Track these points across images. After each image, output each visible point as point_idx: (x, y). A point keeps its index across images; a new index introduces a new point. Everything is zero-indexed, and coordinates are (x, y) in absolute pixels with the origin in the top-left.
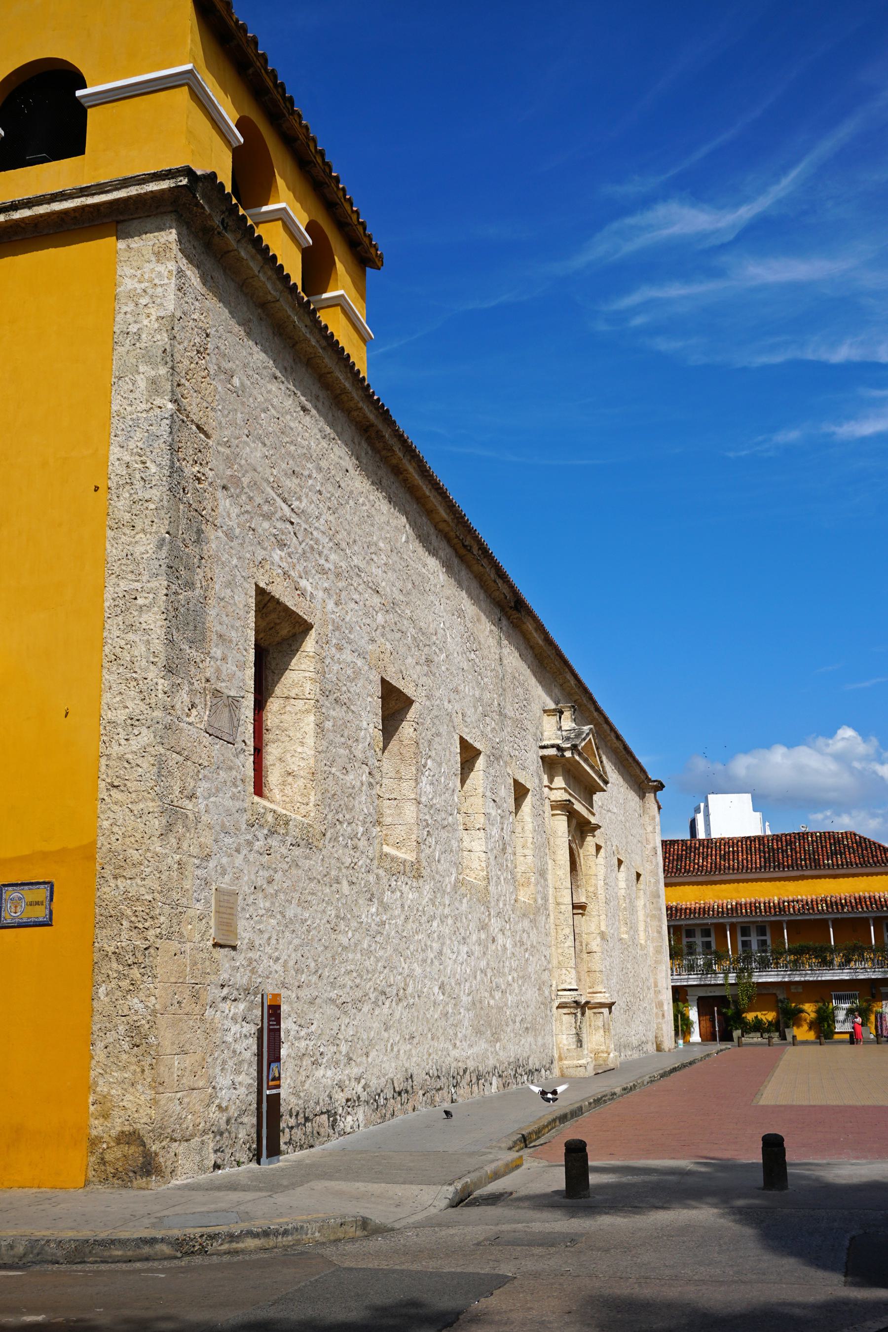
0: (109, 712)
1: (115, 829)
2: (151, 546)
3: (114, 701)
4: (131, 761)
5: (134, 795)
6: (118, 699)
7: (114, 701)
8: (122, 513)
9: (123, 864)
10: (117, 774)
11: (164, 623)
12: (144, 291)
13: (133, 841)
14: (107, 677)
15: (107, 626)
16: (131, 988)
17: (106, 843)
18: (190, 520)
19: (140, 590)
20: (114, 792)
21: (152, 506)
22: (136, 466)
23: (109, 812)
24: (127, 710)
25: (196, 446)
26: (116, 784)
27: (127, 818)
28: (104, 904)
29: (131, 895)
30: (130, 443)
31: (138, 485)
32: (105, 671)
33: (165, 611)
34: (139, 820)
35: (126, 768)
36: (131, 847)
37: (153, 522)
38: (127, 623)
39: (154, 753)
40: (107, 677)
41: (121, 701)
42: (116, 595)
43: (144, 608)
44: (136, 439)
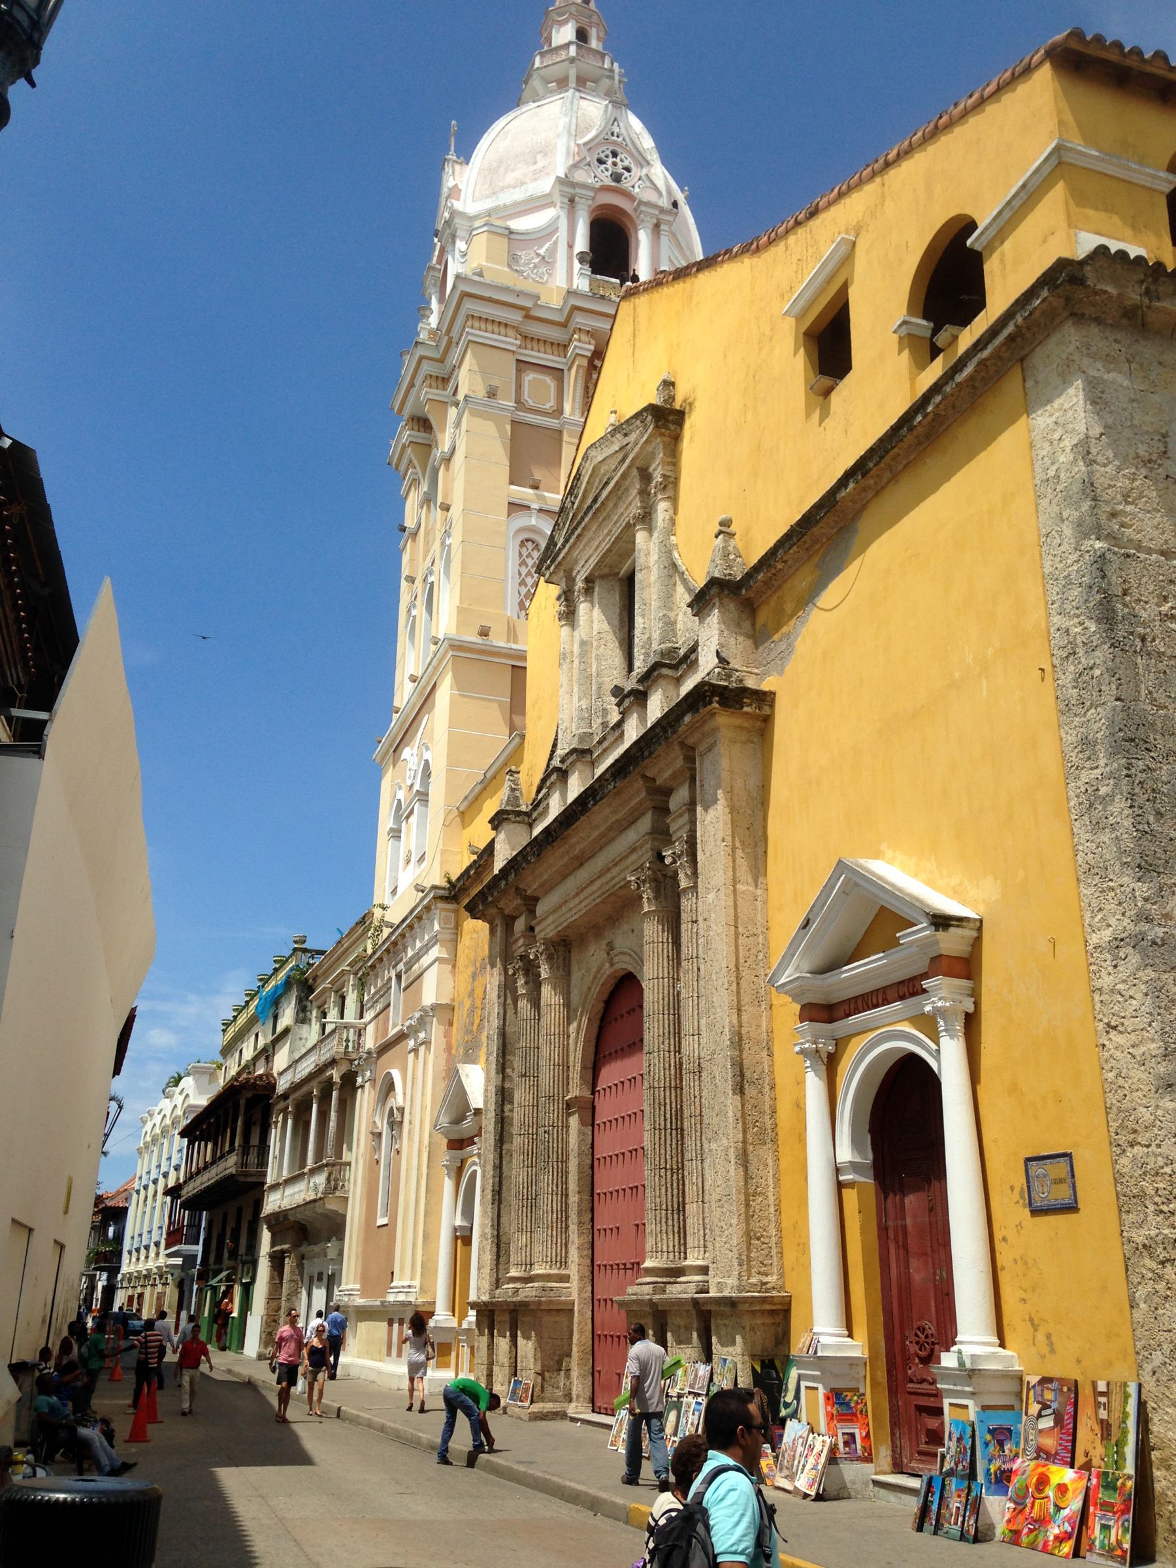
0: (1094, 935)
1: (1121, 1081)
2: (1103, 721)
3: (1096, 919)
4: (1124, 993)
5: (1133, 1036)
6: (1099, 917)
7: (1096, 919)
8: (1070, 691)
9: (1136, 1127)
10: (1113, 1011)
11: (1131, 811)
12: (1056, 423)
13: (1141, 1096)
14: (1085, 891)
15: (1075, 830)
16: (1168, 1293)
17: (1115, 1102)
18: (1165, 672)
19: (1100, 778)
20: (1113, 1034)
21: (1097, 672)
22: (1076, 630)
23: (1111, 1060)
24: (1111, 929)
25: (1161, 578)
26: (1113, 1023)
27: (1130, 1067)
28: (1124, 1180)
29: (1149, 1167)
30: (1065, 606)
31: (1081, 651)
32: (1082, 885)
33: (1129, 796)
34: (1143, 1068)
35: (1119, 1002)
36: (1140, 1105)
37: (1100, 691)
38: (1094, 822)
39: (1145, 979)
40: (1085, 891)
41: (1103, 919)
42: (1079, 791)
43: (1107, 799)
44: (1071, 598)
